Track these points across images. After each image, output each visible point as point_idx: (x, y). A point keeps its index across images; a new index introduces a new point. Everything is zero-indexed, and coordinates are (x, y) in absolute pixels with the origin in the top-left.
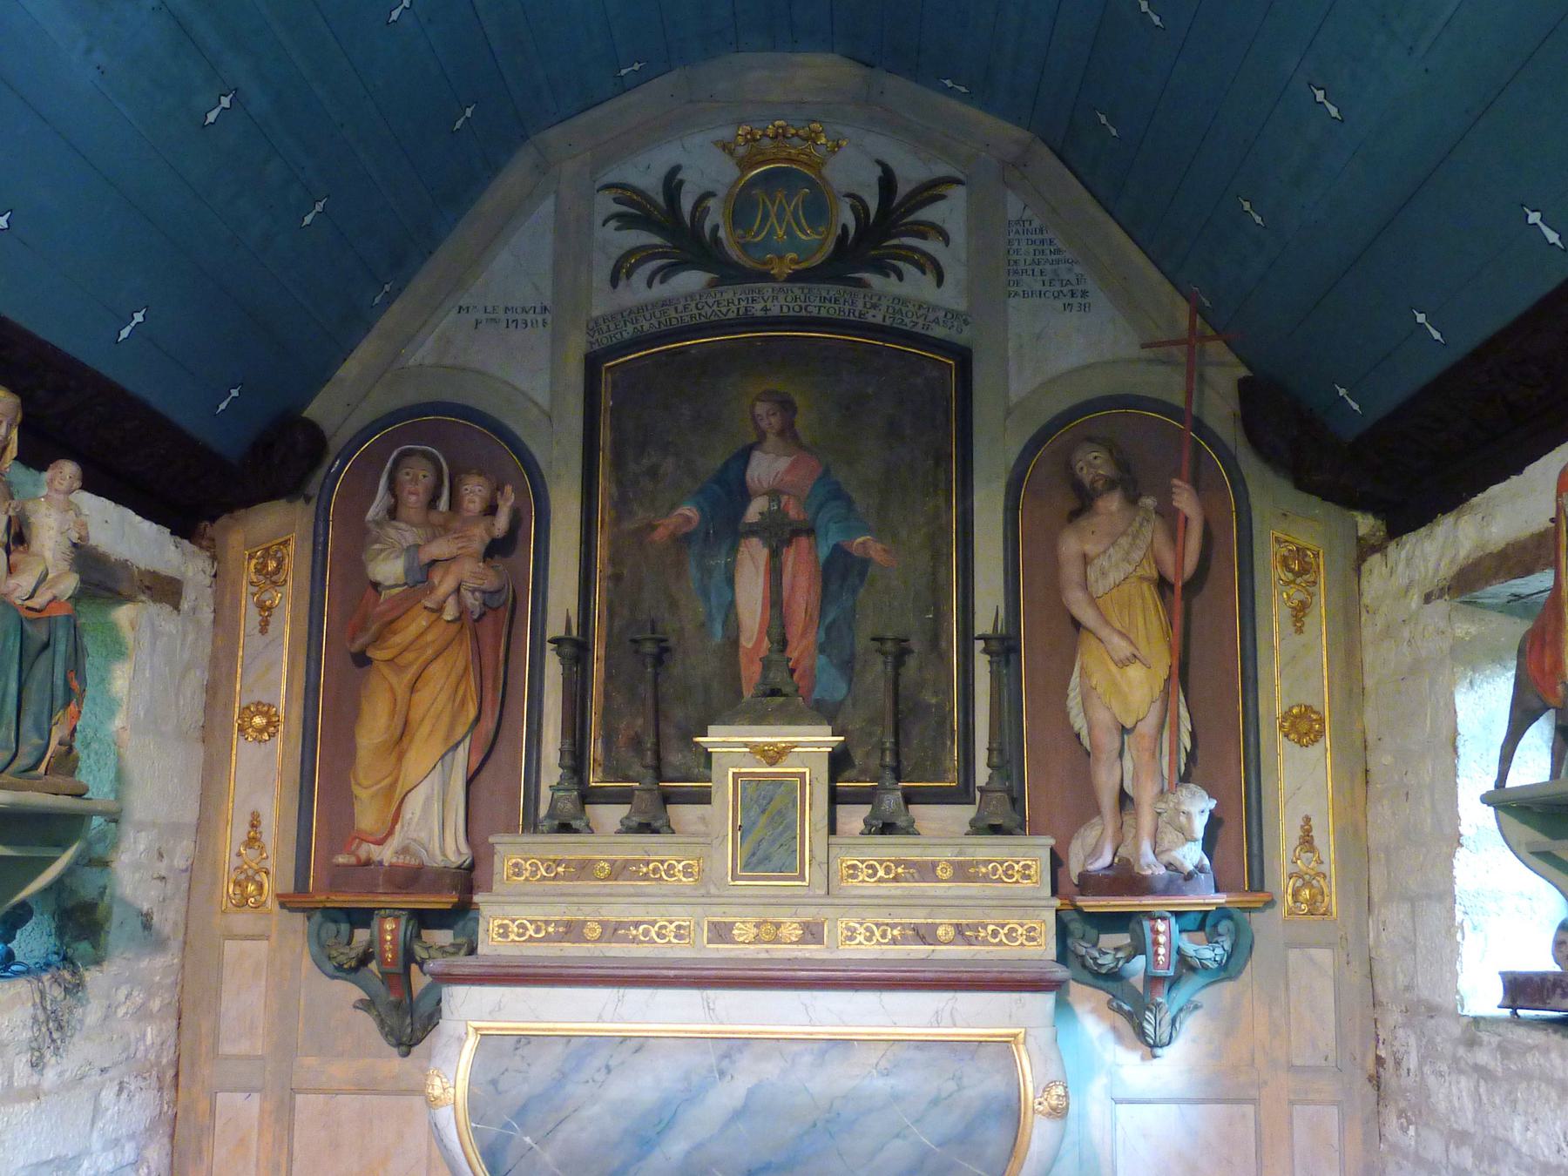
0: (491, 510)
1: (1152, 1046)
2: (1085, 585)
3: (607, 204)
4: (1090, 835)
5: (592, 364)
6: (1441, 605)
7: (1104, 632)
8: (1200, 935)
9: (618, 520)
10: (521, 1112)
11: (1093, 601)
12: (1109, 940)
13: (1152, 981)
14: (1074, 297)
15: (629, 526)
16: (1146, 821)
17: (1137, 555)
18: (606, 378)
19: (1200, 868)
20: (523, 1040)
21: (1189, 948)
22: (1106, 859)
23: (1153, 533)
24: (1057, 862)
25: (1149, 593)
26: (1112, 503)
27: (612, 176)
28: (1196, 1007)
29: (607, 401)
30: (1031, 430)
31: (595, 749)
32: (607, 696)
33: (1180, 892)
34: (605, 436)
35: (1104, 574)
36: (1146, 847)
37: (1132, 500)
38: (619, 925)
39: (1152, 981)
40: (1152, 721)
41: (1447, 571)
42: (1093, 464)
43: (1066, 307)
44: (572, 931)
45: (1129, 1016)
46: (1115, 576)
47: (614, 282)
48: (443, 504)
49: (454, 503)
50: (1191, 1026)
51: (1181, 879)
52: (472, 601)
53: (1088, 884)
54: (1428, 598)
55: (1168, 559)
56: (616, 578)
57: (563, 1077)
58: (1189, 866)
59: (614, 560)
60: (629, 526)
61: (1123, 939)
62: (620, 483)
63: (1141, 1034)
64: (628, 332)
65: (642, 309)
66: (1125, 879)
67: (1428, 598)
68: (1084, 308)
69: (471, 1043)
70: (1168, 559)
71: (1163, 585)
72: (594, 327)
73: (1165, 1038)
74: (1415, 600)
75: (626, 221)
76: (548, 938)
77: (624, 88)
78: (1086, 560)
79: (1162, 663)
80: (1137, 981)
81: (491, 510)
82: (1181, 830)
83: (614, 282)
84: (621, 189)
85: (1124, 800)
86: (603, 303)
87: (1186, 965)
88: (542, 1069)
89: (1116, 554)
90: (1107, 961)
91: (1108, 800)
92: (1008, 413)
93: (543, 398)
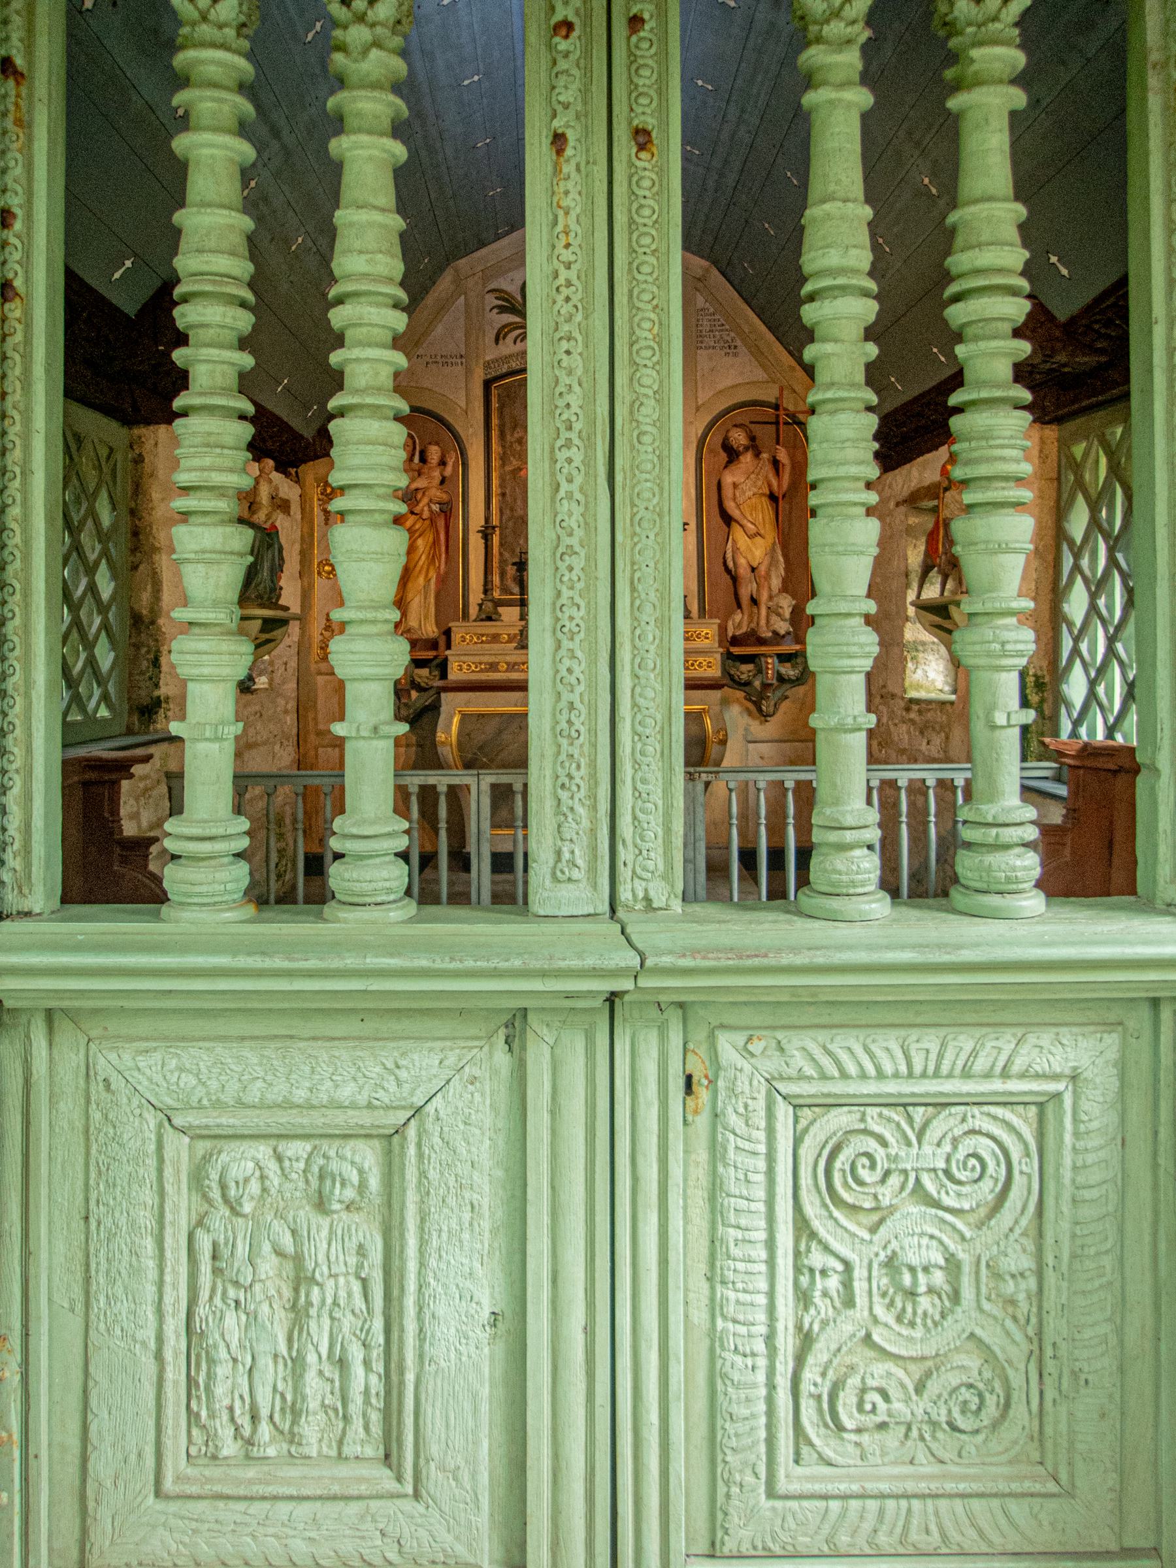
0: (443, 463)
1: (764, 716)
2: (734, 499)
3: (491, 300)
4: (738, 617)
5: (487, 384)
6: (903, 509)
7: (745, 522)
8: (788, 665)
9: (503, 465)
10: (481, 748)
11: (738, 506)
12: (746, 668)
13: (766, 686)
14: (731, 348)
15: (508, 468)
16: (764, 611)
17: (760, 483)
18: (494, 392)
19: (788, 633)
20: (481, 716)
21: (783, 670)
22: (744, 629)
23: (768, 470)
24: (723, 629)
25: (765, 501)
26: (747, 458)
27: (492, 286)
28: (786, 698)
29: (495, 404)
30: (708, 418)
31: (496, 579)
32: (501, 554)
33: (778, 644)
34: (495, 421)
35: (744, 492)
36: (763, 622)
37: (757, 455)
38: (515, 664)
39: (766, 686)
40: (766, 563)
41: (906, 493)
42: (739, 438)
43: (727, 354)
44: (493, 667)
45: (754, 703)
46: (750, 493)
47: (497, 341)
48: (416, 459)
49: (423, 460)
50: (785, 706)
51: (778, 638)
52: (436, 508)
53: (735, 641)
54: (898, 504)
55: (775, 483)
56: (503, 495)
57: (500, 732)
58: (782, 632)
59: (502, 485)
60: (508, 468)
61: (751, 667)
62: (503, 447)
63: (760, 710)
64: (505, 369)
65: (511, 356)
66: (753, 637)
67: (898, 504)
68: (735, 355)
69: (456, 720)
70: (775, 483)
71: (773, 498)
72: (487, 365)
73: (771, 709)
74: (892, 505)
75: (502, 310)
76: (481, 671)
77: (498, 238)
78: (735, 486)
79: (771, 535)
80: (757, 683)
81: (443, 463)
82: (779, 615)
83: (497, 341)
84: (499, 292)
85: (754, 601)
86: (492, 353)
87: (781, 679)
88: (491, 728)
89: (749, 482)
90: (744, 677)
91: (745, 601)
92: (698, 409)
93: (463, 404)
